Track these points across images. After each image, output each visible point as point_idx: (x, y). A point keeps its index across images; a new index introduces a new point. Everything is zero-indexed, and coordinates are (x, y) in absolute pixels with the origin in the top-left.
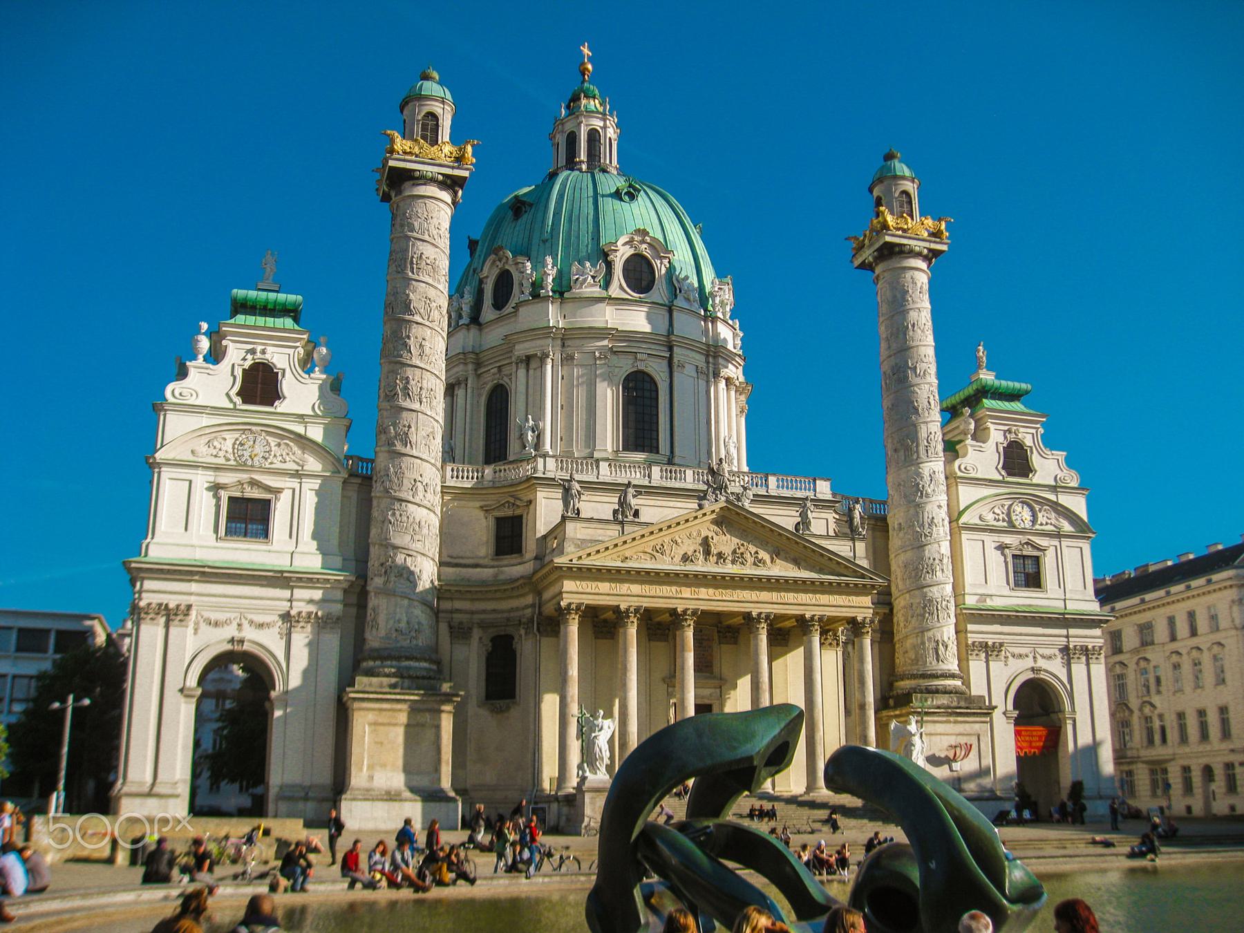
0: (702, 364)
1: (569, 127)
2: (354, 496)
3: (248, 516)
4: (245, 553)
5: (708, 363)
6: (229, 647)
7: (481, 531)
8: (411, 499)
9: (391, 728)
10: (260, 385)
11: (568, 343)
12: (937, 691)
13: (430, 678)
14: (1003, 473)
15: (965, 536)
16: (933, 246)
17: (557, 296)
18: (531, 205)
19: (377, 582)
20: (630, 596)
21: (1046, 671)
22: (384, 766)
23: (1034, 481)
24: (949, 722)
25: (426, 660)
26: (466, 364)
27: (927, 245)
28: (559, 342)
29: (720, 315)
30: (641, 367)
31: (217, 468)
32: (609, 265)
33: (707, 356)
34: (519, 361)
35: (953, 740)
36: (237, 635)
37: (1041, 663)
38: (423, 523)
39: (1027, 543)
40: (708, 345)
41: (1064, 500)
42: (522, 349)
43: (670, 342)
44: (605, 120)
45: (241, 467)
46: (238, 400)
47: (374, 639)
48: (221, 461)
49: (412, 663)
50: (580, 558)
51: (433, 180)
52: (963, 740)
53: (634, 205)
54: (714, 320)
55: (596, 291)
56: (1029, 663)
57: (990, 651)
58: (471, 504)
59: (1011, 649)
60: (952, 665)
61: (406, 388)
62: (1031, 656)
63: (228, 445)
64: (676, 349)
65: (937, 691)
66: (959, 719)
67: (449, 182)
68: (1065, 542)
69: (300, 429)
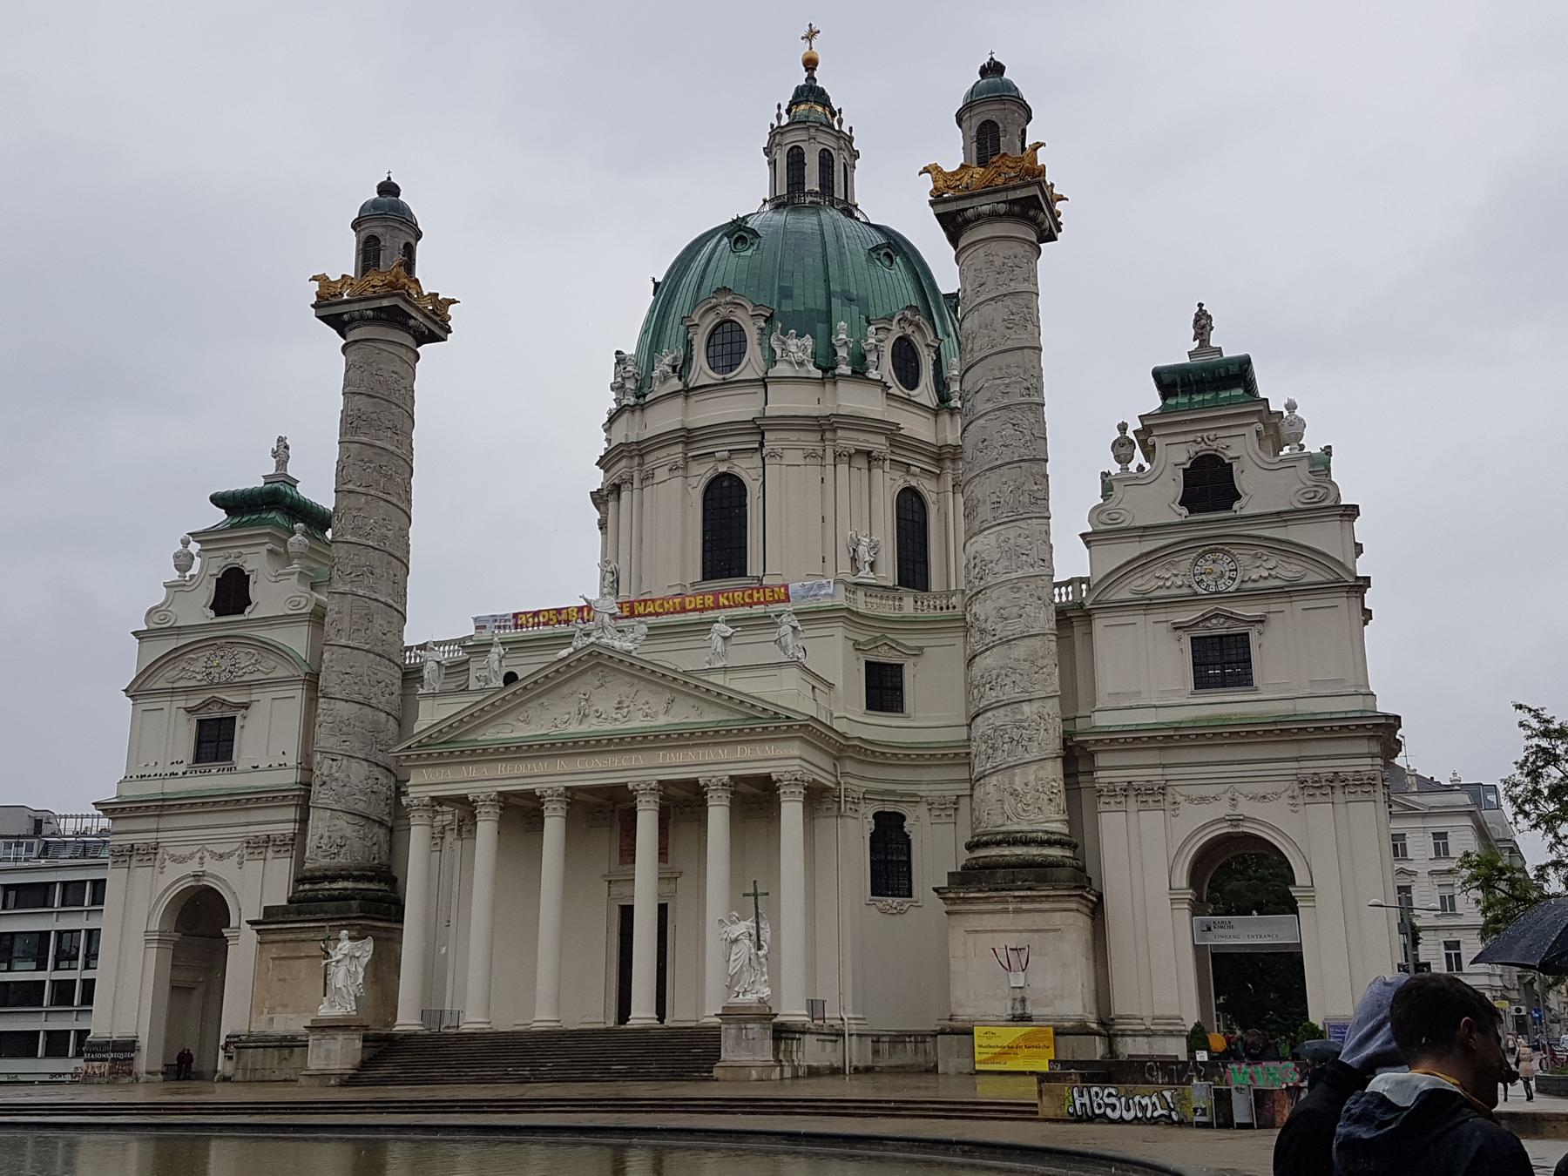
0: (818, 447)
10: (232, 592)
11: (648, 459)
14: (1185, 511)
15: (1099, 624)
16: (1012, 195)
17: (641, 401)
21: (1253, 820)
23: (1245, 512)
24: (1006, 911)
25: (345, 878)
27: (1002, 196)
30: (723, 468)
32: (689, 344)
35: (1013, 941)
37: (1245, 808)
41: (1299, 533)
45: (212, 685)
46: (212, 614)
54: (835, 379)
55: (675, 384)
56: (1222, 809)
57: (1153, 794)
59: (1184, 790)
63: (199, 666)
66: (1024, 906)
68: (1300, 604)
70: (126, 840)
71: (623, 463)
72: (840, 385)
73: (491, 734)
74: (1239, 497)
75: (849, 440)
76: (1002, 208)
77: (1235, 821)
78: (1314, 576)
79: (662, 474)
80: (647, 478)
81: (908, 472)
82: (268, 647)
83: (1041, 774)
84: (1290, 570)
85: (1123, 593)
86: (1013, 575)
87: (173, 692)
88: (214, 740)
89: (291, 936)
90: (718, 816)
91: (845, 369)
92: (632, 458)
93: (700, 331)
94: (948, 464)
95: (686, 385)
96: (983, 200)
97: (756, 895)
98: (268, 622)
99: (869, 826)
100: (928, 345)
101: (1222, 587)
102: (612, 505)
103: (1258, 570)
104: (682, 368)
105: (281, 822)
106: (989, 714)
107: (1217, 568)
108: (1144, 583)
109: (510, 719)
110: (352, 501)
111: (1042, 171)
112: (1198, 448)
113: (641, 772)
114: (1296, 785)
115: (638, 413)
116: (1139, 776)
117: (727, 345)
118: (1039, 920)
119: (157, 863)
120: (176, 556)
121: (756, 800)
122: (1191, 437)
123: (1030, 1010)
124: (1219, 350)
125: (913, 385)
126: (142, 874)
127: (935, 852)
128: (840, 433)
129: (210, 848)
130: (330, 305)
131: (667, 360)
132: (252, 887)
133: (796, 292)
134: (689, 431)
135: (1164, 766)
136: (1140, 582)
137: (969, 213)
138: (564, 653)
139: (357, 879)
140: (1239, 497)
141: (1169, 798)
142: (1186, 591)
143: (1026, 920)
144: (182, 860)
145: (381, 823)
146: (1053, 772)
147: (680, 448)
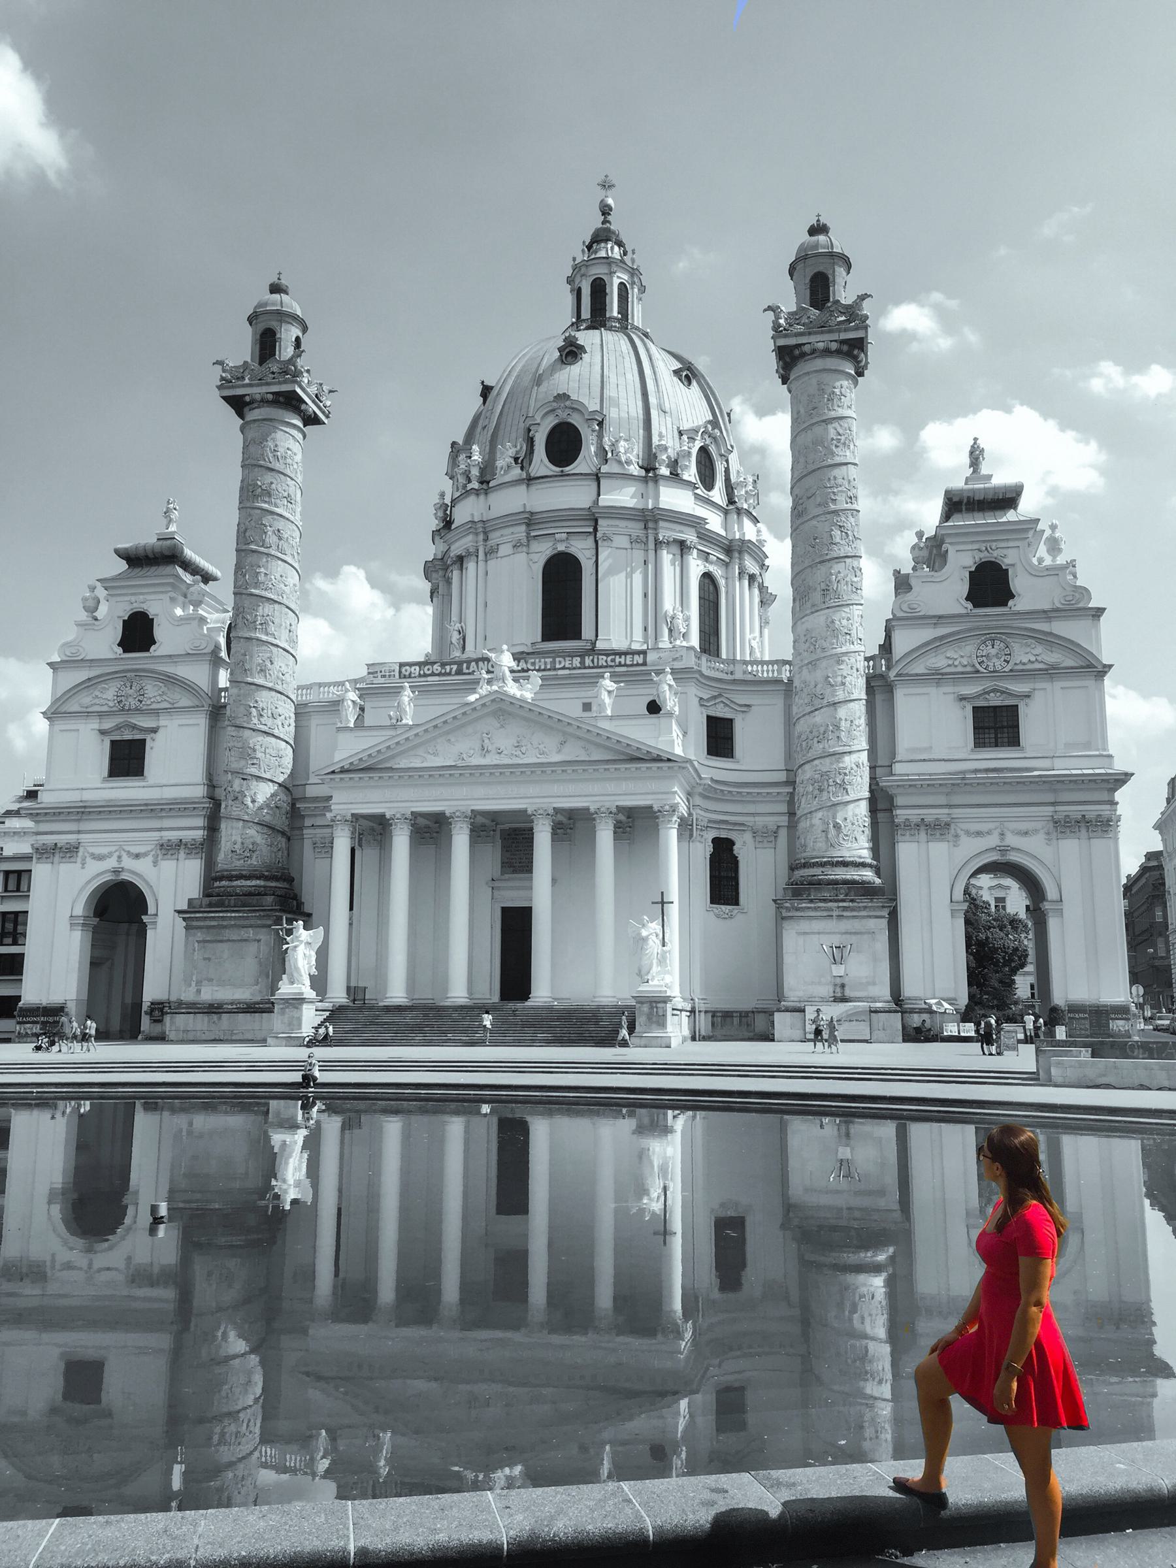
4: (127, 790)
5: (646, 528)
6: (108, 877)
8: (245, 725)
9: (220, 944)
10: (138, 633)
11: (491, 536)
12: (819, 883)
13: (259, 894)
14: (970, 605)
15: (900, 694)
16: (844, 336)
17: (485, 486)
20: (395, 801)
22: (211, 980)
26: (436, 571)
27: (835, 336)
28: (481, 537)
29: (664, 471)
30: (561, 548)
31: (101, 715)
32: (531, 442)
34: (454, 563)
36: (115, 864)
37: (1012, 840)
38: (257, 747)
39: (994, 691)
41: (1060, 628)
42: (457, 549)
43: (593, 514)
44: (609, 264)
46: (120, 650)
47: (223, 859)
48: (105, 708)
50: (343, 771)
51: (264, 402)
54: (656, 479)
55: (516, 472)
56: (993, 841)
57: (938, 829)
61: (243, 618)
62: (996, 834)
64: (600, 522)
66: (845, 914)
67: (281, 399)
68: (1058, 685)
69: (170, 669)
70: (50, 839)
71: (470, 537)
72: (661, 482)
73: (403, 763)
74: (1013, 596)
76: (834, 346)
77: (1003, 850)
78: (1069, 663)
79: (505, 549)
80: (491, 552)
81: (707, 560)
82: (171, 681)
83: (857, 811)
84: (1054, 657)
85: (919, 668)
86: (839, 650)
88: (127, 759)
89: (213, 923)
90: (605, 837)
91: (664, 471)
92: (477, 534)
93: (541, 429)
94: (736, 555)
95: (528, 474)
96: (819, 337)
97: (663, 903)
99: (710, 849)
100: (721, 455)
101: (999, 668)
102: (455, 575)
103: (1024, 654)
105: (193, 829)
106: (816, 762)
107: (993, 652)
108: (938, 661)
109: (420, 751)
110: (251, 559)
111: (867, 317)
112: (982, 555)
113: (537, 799)
114: (1051, 825)
115: (482, 497)
116: (930, 815)
117: (564, 444)
118: (856, 925)
119: (79, 860)
120: (85, 599)
121: (636, 825)
122: (976, 546)
123: (848, 993)
124: (990, 477)
125: (709, 486)
127: (759, 871)
128: (661, 524)
129: (127, 848)
130: (233, 387)
131: (512, 452)
132: (171, 885)
133: (623, 401)
134: (532, 513)
135: (950, 806)
136: (933, 660)
137: (807, 348)
138: (472, 698)
139: (266, 878)
140: (1013, 596)
141: (952, 831)
142: (969, 669)
143: (845, 925)
144: (100, 858)
145: (283, 833)
146: (863, 808)
147: (523, 528)
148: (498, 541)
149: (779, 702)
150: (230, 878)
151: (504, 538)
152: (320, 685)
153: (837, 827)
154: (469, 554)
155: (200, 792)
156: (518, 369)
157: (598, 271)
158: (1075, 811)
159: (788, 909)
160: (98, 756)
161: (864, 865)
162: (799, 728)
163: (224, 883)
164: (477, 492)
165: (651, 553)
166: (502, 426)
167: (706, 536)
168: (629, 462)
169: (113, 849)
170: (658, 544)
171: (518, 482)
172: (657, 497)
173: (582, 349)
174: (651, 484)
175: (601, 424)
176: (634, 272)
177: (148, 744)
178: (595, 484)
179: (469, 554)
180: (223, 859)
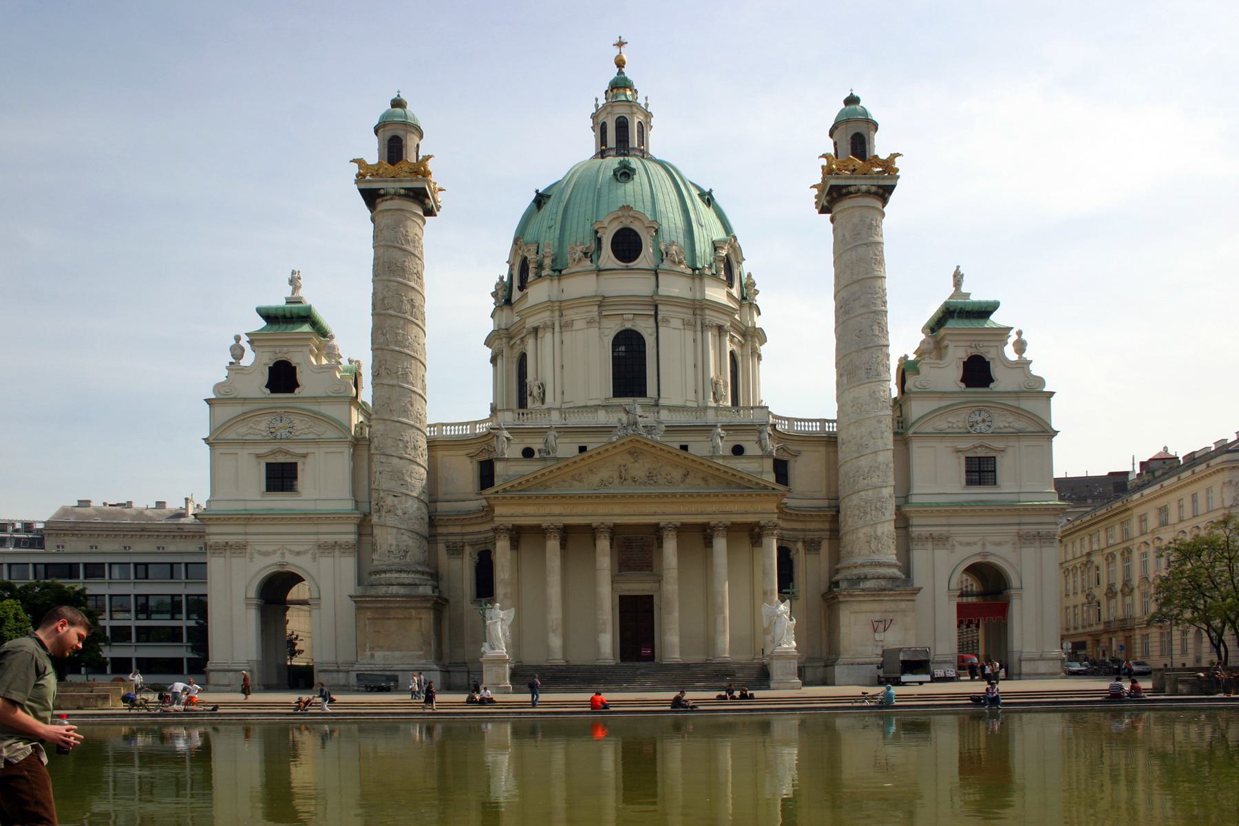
1: (601, 120)
2: (365, 454)
3: (281, 477)
4: (281, 502)
7: (464, 473)
12: (866, 578)
18: (549, 197)
19: (375, 519)
28: (557, 313)
29: (707, 272)
30: (628, 326)
32: (599, 241)
33: (694, 309)
34: (529, 333)
35: (878, 617)
40: (694, 300)
49: (404, 575)
52: (891, 616)
53: (629, 186)
55: (587, 263)
58: (460, 453)
60: (891, 556)
64: (660, 307)
65: (866, 578)
71: (548, 313)
75: (712, 317)
79: (580, 324)
85: (928, 428)
87: (244, 443)
93: (608, 231)
98: (316, 399)
102: (530, 342)
104: (591, 254)
115: (556, 282)
116: (936, 531)
117: (627, 245)
118: (892, 606)
125: (731, 286)
126: (237, 562)
128: (707, 312)
139: (419, 572)
147: (596, 308)
148: (574, 317)
149: (822, 449)
150: (391, 571)
151: (578, 316)
152: (443, 424)
153: (876, 538)
154: (545, 327)
155: (348, 505)
156: (574, 180)
157: (621, 111)
158: (1032, 529)
159: (845, 596)
160: (258, 476)
161: (895, 566)
162: (842, 470)
163: (383, 575)
164: (551, 277)
165: (699, 333)
166: (568, 227)
167: (734, 326)
168: (680, 263)
169: (276, 548)
170: (704, 327)
171: (590, 272)
172: (703, 292)
173: (633, 170)
174: (697, 281)
175: (656, 231)
176: (648, 115)
177: (300, 467)
178: (653, 278)
179: (545, 327)
180: (378, 559)
